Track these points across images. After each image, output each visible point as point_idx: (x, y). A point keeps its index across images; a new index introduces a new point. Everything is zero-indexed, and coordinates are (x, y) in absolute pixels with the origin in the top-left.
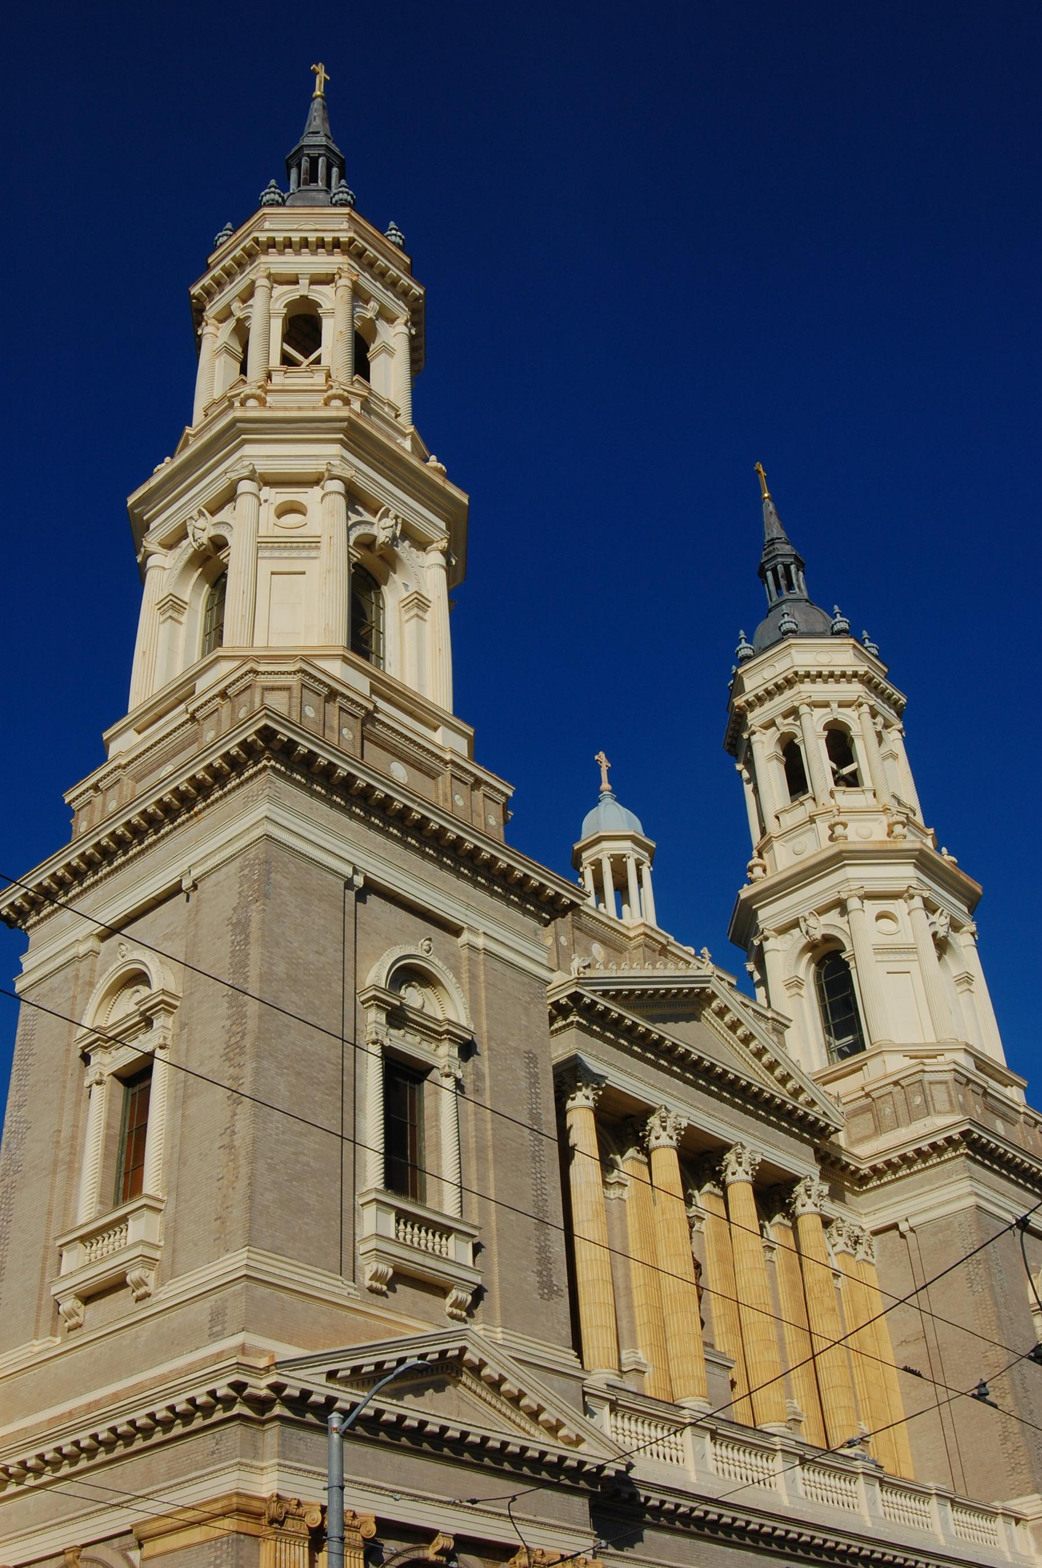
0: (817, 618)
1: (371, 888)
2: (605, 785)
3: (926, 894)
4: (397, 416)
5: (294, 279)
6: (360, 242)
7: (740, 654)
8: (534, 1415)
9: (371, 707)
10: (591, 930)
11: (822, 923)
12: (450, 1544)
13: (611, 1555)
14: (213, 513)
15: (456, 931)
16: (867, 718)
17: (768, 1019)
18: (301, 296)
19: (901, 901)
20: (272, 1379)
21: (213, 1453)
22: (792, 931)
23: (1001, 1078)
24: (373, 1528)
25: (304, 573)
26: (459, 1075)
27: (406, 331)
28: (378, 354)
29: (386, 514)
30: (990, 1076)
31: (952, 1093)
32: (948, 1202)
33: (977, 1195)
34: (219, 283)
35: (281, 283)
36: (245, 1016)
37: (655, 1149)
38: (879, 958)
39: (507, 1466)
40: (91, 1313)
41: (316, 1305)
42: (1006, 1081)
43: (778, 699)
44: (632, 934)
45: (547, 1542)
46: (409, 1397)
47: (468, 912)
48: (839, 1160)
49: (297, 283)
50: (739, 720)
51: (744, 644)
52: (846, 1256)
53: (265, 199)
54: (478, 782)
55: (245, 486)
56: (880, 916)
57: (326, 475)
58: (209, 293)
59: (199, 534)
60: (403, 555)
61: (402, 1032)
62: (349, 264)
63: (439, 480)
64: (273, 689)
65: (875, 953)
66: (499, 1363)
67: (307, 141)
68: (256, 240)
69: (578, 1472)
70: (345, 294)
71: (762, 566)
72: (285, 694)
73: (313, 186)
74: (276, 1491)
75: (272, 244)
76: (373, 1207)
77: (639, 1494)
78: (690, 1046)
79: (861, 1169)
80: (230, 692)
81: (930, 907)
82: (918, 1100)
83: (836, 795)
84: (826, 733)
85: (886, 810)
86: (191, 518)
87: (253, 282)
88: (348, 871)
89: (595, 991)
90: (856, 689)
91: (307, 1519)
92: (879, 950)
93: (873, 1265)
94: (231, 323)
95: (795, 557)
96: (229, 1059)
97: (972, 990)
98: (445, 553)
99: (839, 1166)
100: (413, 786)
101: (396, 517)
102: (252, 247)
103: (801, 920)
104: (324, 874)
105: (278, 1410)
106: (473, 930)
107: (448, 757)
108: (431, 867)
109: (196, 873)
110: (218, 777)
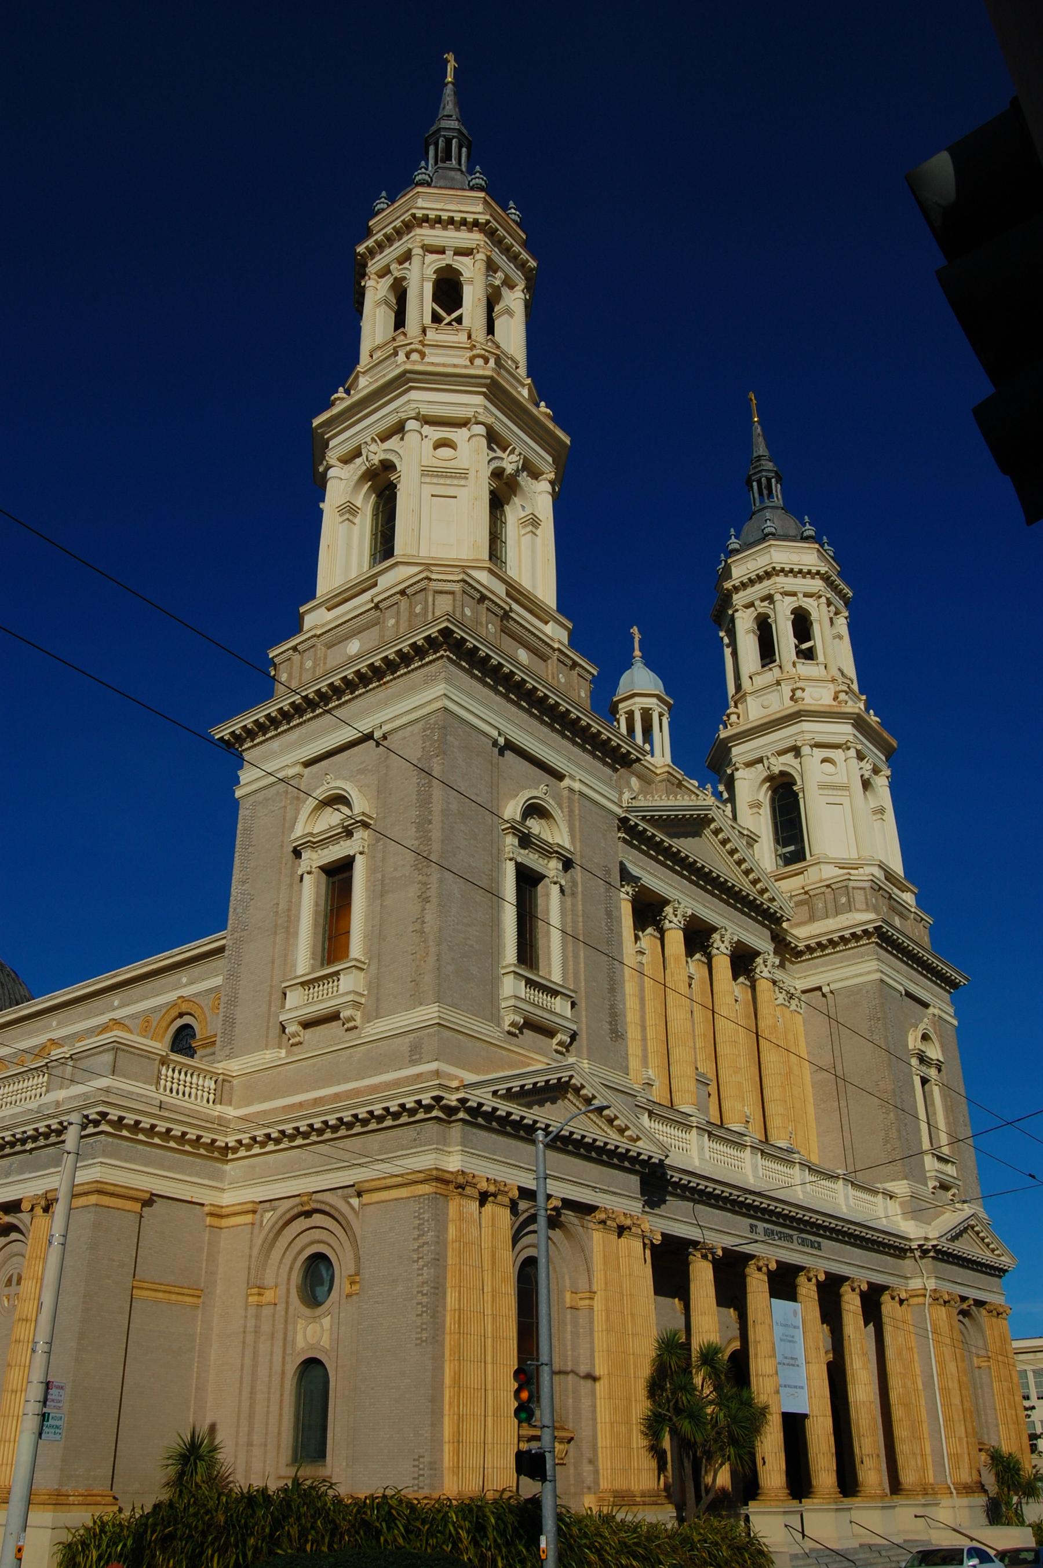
0: (790, 524)
1: (510, 746)
2: (637, 653)
3: (859, 747)
4: (517, 368)
5: (441, 249)
6: (494, 224)
7: (730, 547)
8: (610, 1121)
9: (508, 608)
11: (781, 762)
12: (559, 1204)
14: (383, 440)
15: (560, 777)
16: (824, 607)
17: (744, 835)
18: (447, 265)
19: (840, 750)
20: (461, 1095)
21: (415, 1140)
22: (757, 766)
23: (900, 885)
24: (516, 1193)
25: (456, 497)
26: (563, 883)
27: (523, 296)
28: (500, 316)
29: (512, 452)
30: (894, 885)
31: (869, 897)
32: (861, 975)
33: (882, 972)
34: (380, 246)
35: (431, 252)
36: (430, 840)
37: (668, 930)
38: (821, 792)
39: (594, 1154)
40: (308, 1035)
41: (478, 1044)
42: (904, 888)
43: (758, 587)
44: (658, 771)
45: (615, 1204)
46: (536, 1107)
47: (569, 764)
48: (785, 939)
49: (443, 253)
50: (726, 599)
51: (733, 539)
52: (784, 1007)
53: (417, 178)
54: (575, 664)
55: (411, 425)
56: (823, 761)
57: (473, 420)
58: (371, 252)
59: (371, 456)
60: (523, 483)
61: (527, 851)
62: (485, 242)
63: (551, 425)
64: (441, 592)
65: (819, 789)
66: (592, 1086)
67: (444, 124)
68: (414, 216)
69: (635, 1160)
70: (481, 266)
71: (750, 477)
72: (450, 597)
73: (447, 164)
74: (460, 1168)
75: (426, 219)
76: (512, 976)
77: (666, 1174)
80: (408, 591)
81: (860, 757)
82: (844, 900)
83: (797, 665)
84: (793, 616)
85: (833, 680)
86: (365, 442)
87: (410, 250)
88: (495, 733)
89: (638, 816)
90: (817, 585)
91: (478, 1186)
92: (822, 786)
93: (800, 1014)
94: (388, 281)
95: (776, 473)
96: (419, 870)
97: (884, 818)
98: (552, 483)
99: (783, 943)
100: (534, 668)
101: (520, 454)
102: (410, 220)
103: (765, 758)
104: (480, 736)
105: (461, 1115)
106: (572, 778)
107: (556, 646)
108: (546, 730)
109: (386, 728)
110: (405, 659)
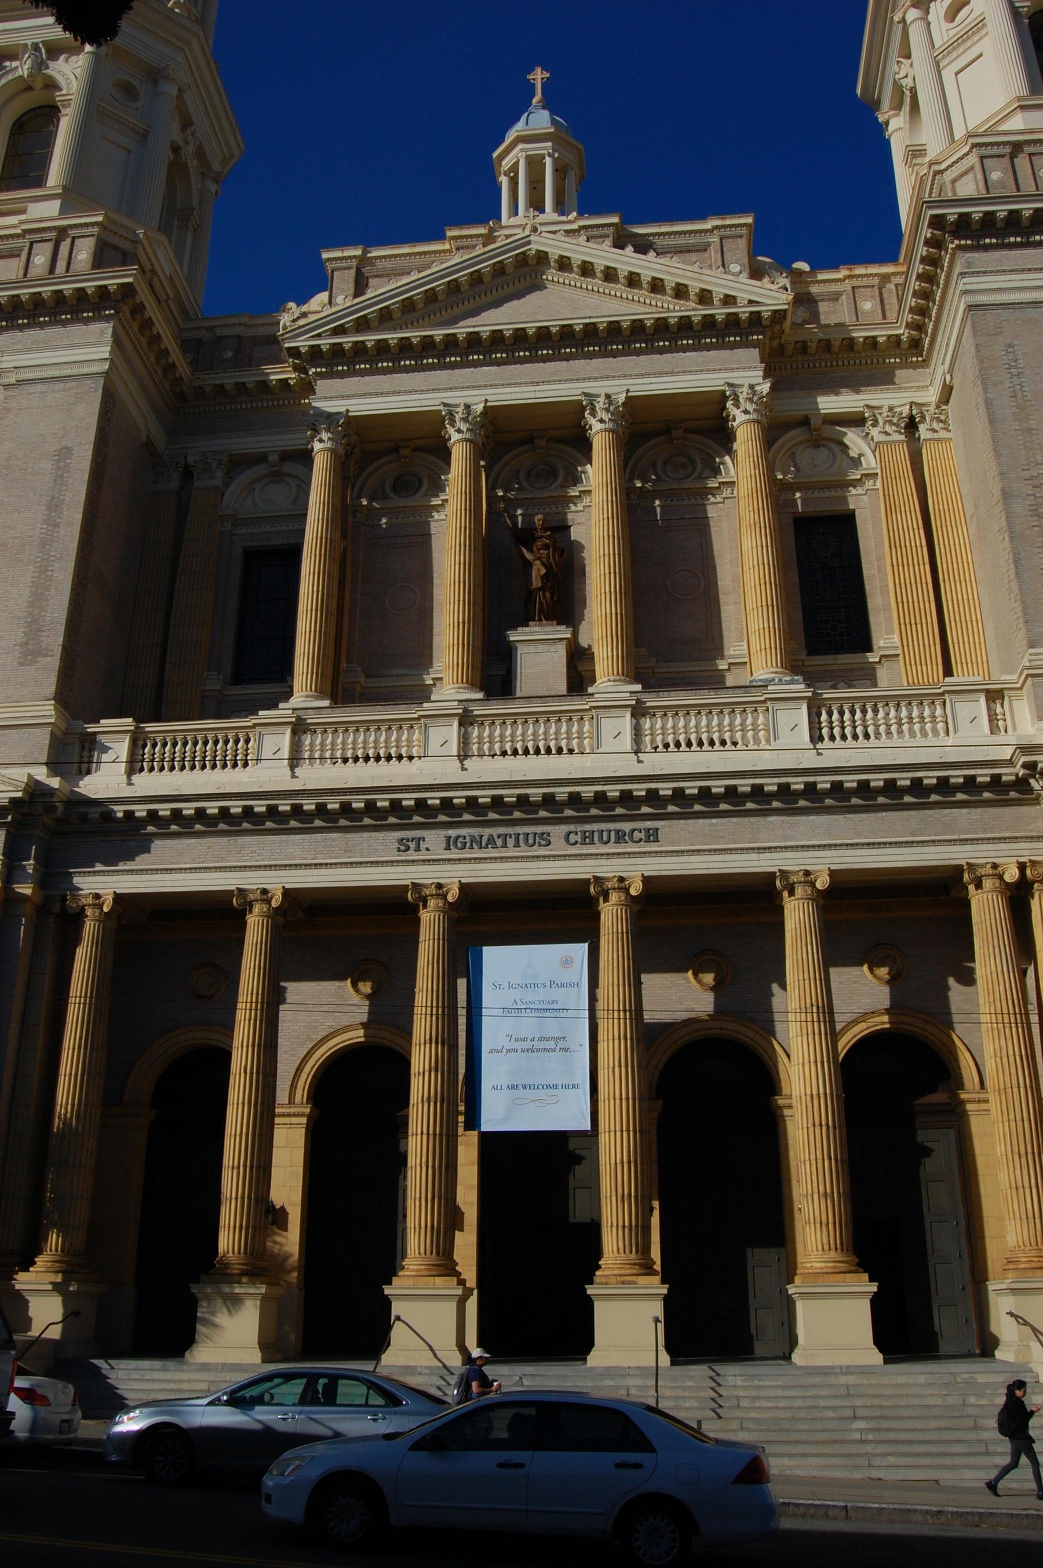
10: (392, 269)
13: (99, 872)
17: (711, 231)
48: (852, 340)
77: (115, 812)
78: (474, 326)
89: (319, 335)
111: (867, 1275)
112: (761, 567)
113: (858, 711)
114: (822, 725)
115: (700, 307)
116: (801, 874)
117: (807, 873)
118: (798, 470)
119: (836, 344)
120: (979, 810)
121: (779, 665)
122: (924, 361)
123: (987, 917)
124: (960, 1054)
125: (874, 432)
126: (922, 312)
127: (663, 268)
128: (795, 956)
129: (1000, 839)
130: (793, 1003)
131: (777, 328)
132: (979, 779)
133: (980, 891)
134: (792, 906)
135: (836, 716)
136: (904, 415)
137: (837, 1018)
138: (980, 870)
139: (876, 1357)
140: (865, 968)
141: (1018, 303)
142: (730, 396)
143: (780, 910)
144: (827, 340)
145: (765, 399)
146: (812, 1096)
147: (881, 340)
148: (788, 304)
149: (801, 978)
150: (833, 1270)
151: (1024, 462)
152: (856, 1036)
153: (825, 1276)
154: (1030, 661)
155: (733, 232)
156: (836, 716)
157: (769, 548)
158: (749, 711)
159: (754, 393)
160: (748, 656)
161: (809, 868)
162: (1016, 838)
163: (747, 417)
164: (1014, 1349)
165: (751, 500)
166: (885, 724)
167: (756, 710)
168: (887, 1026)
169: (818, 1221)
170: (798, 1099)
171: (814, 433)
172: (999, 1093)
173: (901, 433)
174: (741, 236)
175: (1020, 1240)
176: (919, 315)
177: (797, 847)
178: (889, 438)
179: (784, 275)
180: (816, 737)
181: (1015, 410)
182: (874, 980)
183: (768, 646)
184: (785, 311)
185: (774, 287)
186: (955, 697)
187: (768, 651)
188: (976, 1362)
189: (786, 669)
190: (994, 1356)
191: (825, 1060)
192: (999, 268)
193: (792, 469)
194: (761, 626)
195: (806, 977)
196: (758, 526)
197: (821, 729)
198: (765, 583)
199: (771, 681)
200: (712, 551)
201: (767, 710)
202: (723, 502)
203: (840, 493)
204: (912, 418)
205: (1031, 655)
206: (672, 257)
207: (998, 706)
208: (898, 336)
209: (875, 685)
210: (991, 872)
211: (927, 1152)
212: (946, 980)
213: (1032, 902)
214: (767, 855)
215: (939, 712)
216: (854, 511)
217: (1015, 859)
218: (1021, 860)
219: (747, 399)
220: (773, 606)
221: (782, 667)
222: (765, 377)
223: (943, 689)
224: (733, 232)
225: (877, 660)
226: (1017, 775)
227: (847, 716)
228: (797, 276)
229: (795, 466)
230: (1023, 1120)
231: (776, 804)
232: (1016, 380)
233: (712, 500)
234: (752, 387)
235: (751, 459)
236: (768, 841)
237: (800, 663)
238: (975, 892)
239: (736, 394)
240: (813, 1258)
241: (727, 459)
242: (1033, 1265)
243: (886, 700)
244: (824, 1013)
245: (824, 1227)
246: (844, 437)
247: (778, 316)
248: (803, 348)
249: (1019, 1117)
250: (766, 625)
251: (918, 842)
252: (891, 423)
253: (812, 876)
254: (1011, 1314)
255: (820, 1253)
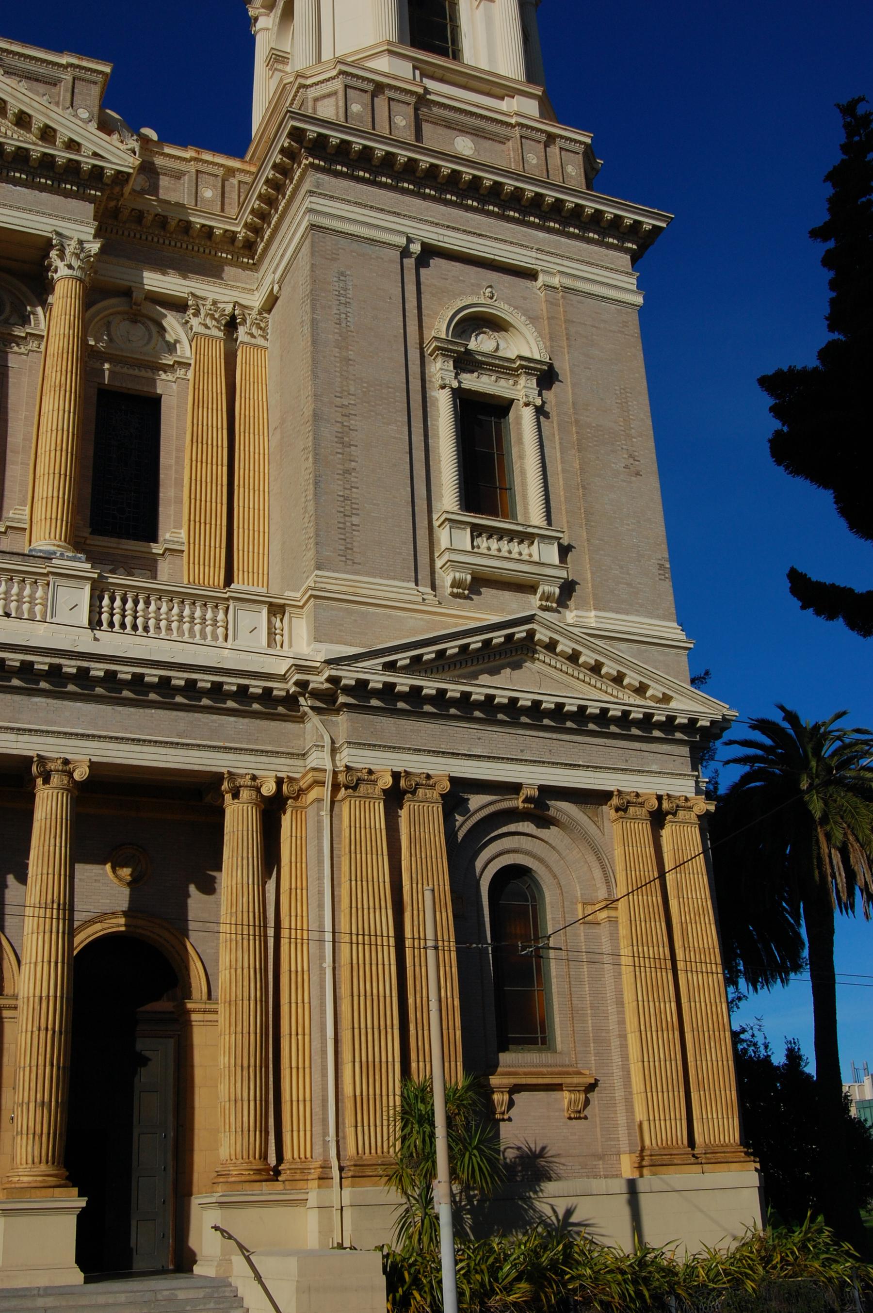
48: (189, 223)
79: (237, 233)
111: (76, 1189)
112: (60, 433)
113: (141, 601)
114: (103, 610)
115: (40, 143)
116: (59, 762)
117: (66, 762)
118: (111, 340)
119: (173, 223)
120: (247, 720)
121: (63, 539)
122: (254, 264)
123: (240, 828)
124: (191, 960)
125: (194, 322)
126: (264, 217)
127: (9, 89)
128: (41, 848)
129: (262, 751)
130: (33, 897)
131: (117, 189)
132: (251, 690)
133: (236, 801)
134: (45, 794)
135: (118, 603)
136: (226, 312)
137: (77, 916)
138: (239, 780)
139: (77, 1277)
140: (108, 867)
141: (357, 236)
142: (56, 246)
143: (31, 798)
144: (164, 216)
145: (92, 259)
146: (41, 998)
147: (218, 232)
148: (134, 168)
149: (45, 872)
150: (42, 1185)
151: (338, 389)
152: (89, 936)
153: (33, 1190)
154: (315, 582)
155: (87, 75)
156: (118, 603)
157: (72, 414)
158: (28, 581)
159: (82, 249)
160: (29, 522)
161: (68, 757)
162: (277, 753)
163: (70, 272)
164: (216, 1264)
165: (60, 360)
166: (167, 619)
167: (36, 583)
168: (123, 929)
169: (31, 1131)
170: (26, 1000)
171: (134, 307)
172: (230, 1005)
173: (220, 330)
174: (95, 83)
175: (233, 1152)
176: (259, 219)
177: (59, 733)
178: (207, 332)
179: (135, 137)
180: (95, 623)
181: (337, 337)
182: (115, 880)
183: (54, 516)
184: (129, 174)
185: (123, 147)
186: (239, 605)
187: (54, 521)
188: (177, 1279)
189: (69, 544)
190: (192, 1271)
191: (60, 960)
192: (344, 197)
193: (105, 337)
194: (50, 495)
195: (51, 871)
196: (63, 389)
197: (101, 613)
198: (61, 450)
199: (52, 554)
200: (7, 403)
201: (48, 584)
202: (27, 355)
203: (149, 374)
204: (233, 317)
205: (317, 576)
206: (20, 81)
207: (278, 619)
208: (234, 233)
209: (154, 577)
210: (249, 783)
211: (144, 1061)
212: (187, 887)
213: (283, 817)
214: (26, 738)
215: (221, 616)
216: (161, 396)
217: (274, 774)
218: (280, 775)
219: (74, 253)
220: (66, 476)
221: (65, 541)
222: (96, 236)
223: (229, 594)
224: (87, 75)
225: (161, 552)
226: (288, 691)
227: (130, 605)
228: (145, 141)
229: (109, 335)
230: (249, 1033)
231: (43, 685)
232: (342, 307)
233: (16, 349)
234: (81, 242)
235: (68, 317)
236: (29, 723)
237: (83, 540)
238: (231, 801)
239: (62, 246)
240: (21, 1171)
241: (39, 310)
242: (243, 1178)
243: (161, 594)
244: (64, 910)
245: (37, 1138)
246: (163, 319)
247: (121, 178)
248: (139, 217)
249: (246, 1030)
250: (55, 494)
251: (183, 744)
252: (213, 317)
253: (71, 766)
254: (216, 1228)
255: (29, 1166)
